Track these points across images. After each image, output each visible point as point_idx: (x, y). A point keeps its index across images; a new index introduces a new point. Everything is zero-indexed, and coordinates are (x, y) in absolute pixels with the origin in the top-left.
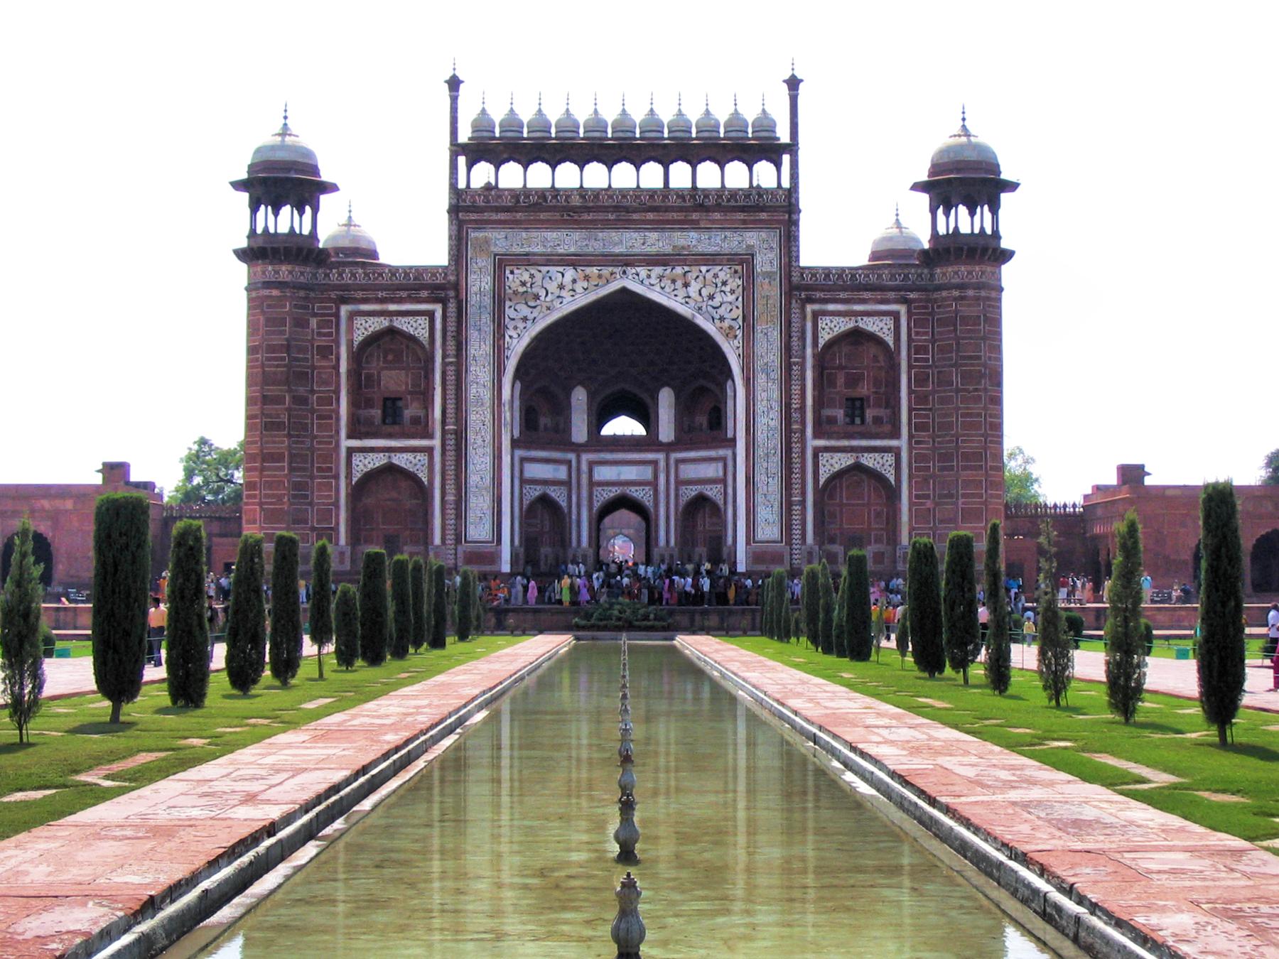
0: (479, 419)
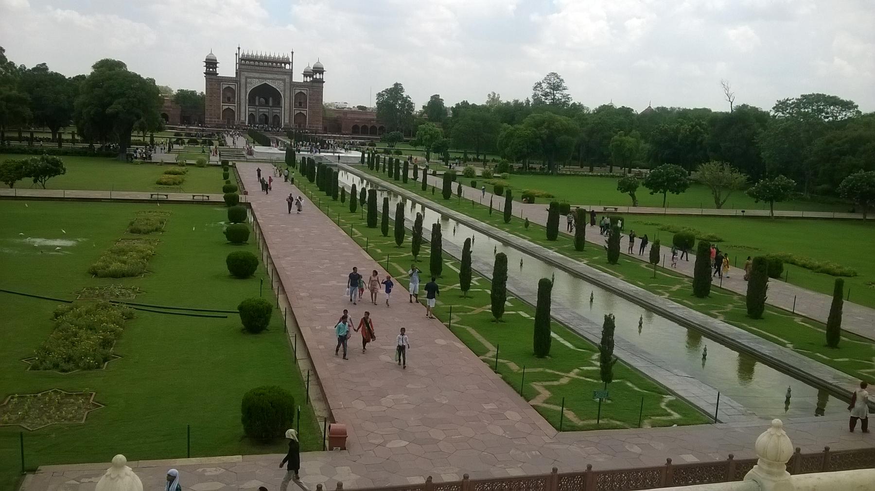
0: (243, 102)
